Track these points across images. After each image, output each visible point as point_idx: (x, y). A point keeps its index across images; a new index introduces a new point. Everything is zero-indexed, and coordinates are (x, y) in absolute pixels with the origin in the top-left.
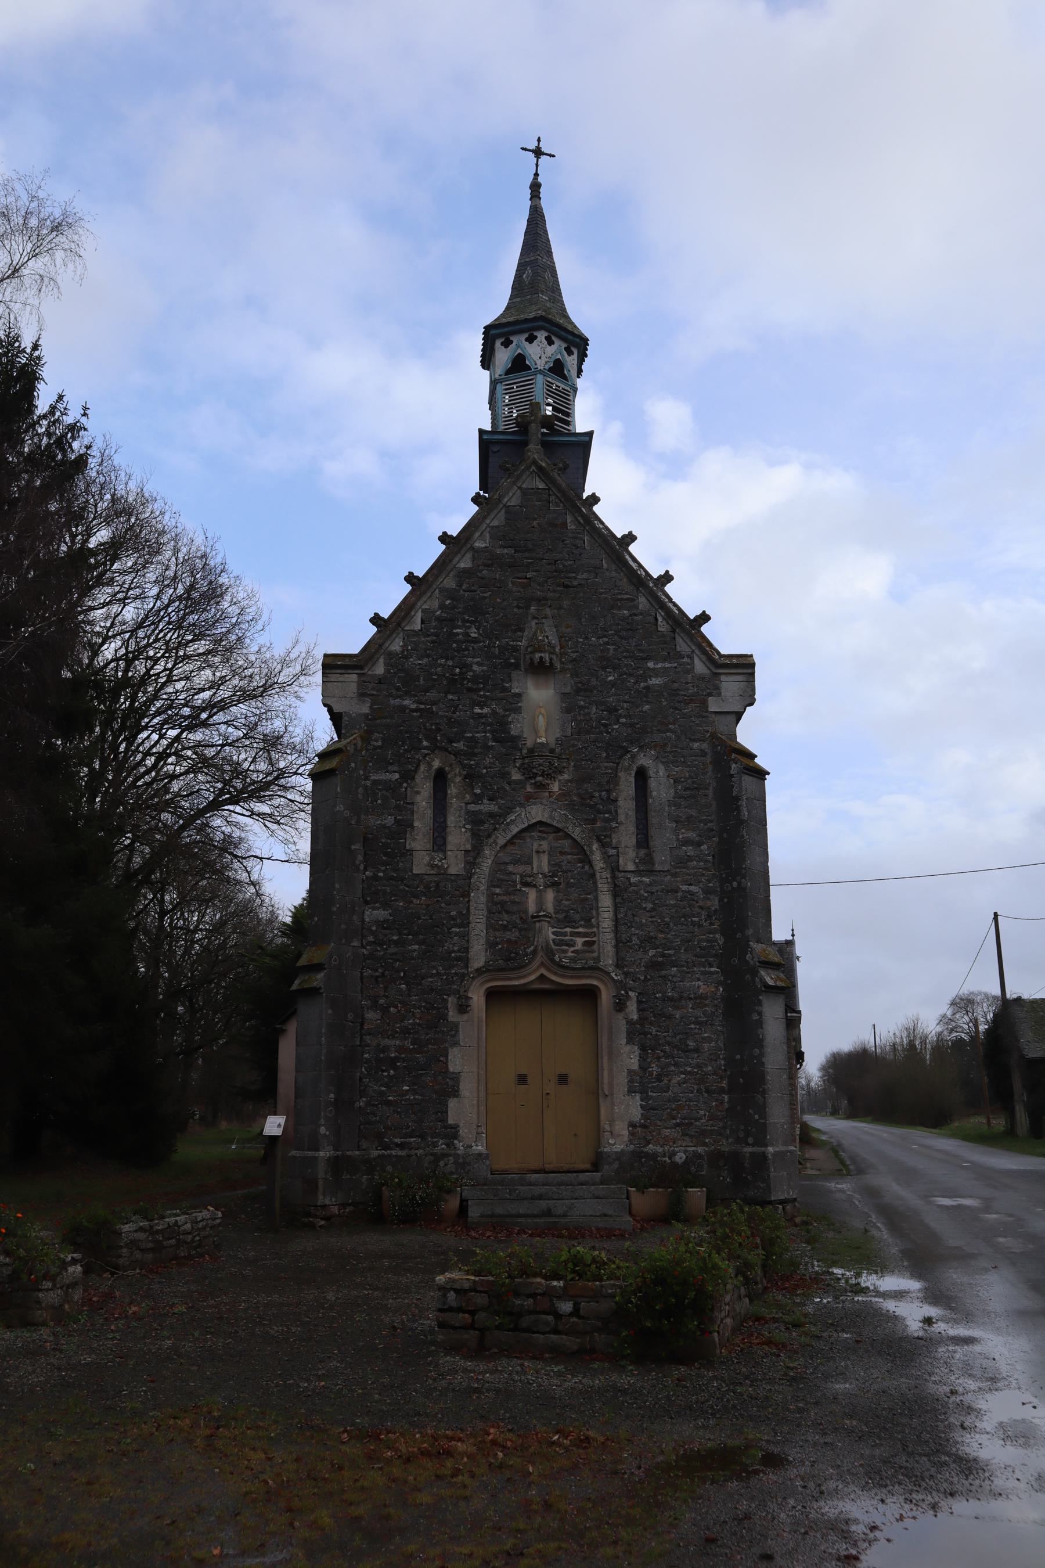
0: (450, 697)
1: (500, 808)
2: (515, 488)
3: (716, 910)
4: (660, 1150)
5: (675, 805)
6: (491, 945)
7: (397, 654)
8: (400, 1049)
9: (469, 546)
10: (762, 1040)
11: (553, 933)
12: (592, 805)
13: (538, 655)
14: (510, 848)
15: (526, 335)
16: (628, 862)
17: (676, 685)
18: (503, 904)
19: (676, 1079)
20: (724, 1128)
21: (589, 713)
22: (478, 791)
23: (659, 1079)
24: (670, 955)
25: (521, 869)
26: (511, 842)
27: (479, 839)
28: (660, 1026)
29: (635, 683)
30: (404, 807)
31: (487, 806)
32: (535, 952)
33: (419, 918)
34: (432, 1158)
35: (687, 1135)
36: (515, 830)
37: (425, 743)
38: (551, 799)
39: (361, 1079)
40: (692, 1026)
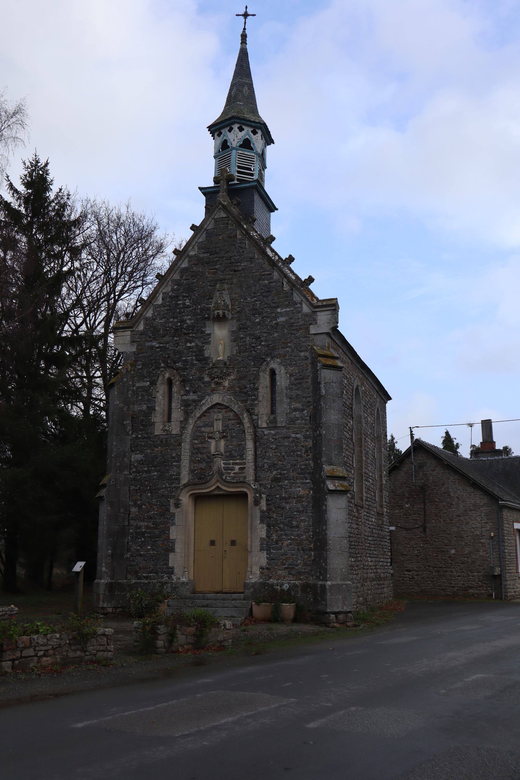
0: (175, 339)
1: (198, 397)
2: (211, 219)
3: (310, 448)
4: (275, 582)
5: (289, 389)
6: (192, 471)
7: (150, 318)
8: (147, 527)
9: (186, 255)
10: (326, 521)
11: (223, 463)
12: (246, 393)
13: (216, 312)
14: (203, 419)
15: (228, 128)
16: (263, 423)
17: (292, 320)
18: (198, 449)
19: (286, 543)
20: (312, 570)
21: (245, 341)
22: (188, 389)
23: (277, 543)
24: (284, 474)
25: (208, 429)
26: (203, 415)
27: (187, 414)
28: (278, 514)
29: (270, 322)
30: (151, 400)
31: (192, 397)
32: (212, 475)
33: (157, 458)
34: (160, 584)
35: (291, 574)
36: (204, 408)
37: (162, 365)
38: (225, 390)
39: (128, 543)
40: (295, 513)
